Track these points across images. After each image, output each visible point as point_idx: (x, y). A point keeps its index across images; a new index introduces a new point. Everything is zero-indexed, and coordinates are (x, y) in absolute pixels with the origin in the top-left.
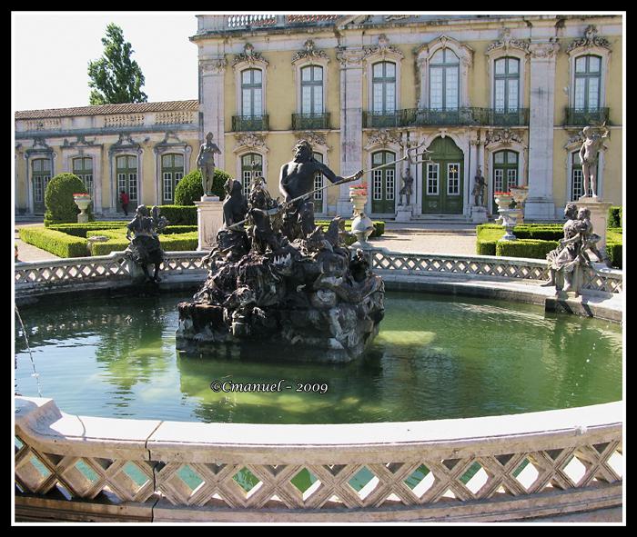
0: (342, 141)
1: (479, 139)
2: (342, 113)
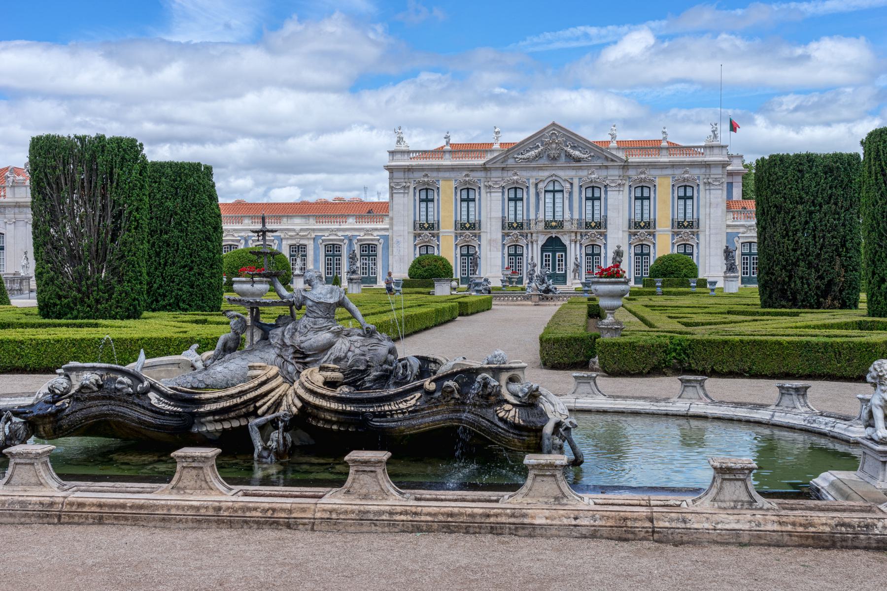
0: (489, 238)
1: (576, 238)
2: (488, 220)
